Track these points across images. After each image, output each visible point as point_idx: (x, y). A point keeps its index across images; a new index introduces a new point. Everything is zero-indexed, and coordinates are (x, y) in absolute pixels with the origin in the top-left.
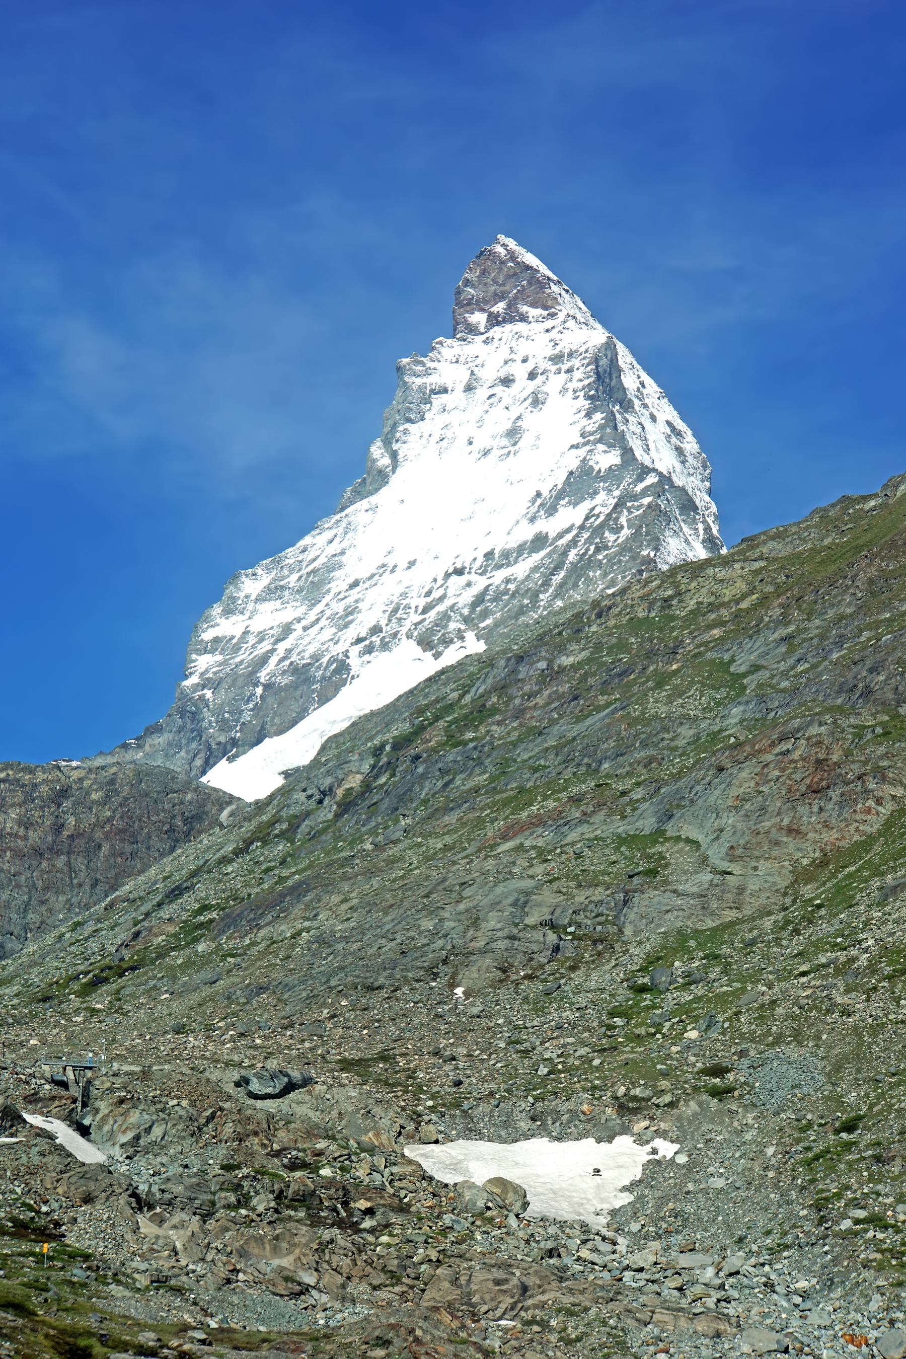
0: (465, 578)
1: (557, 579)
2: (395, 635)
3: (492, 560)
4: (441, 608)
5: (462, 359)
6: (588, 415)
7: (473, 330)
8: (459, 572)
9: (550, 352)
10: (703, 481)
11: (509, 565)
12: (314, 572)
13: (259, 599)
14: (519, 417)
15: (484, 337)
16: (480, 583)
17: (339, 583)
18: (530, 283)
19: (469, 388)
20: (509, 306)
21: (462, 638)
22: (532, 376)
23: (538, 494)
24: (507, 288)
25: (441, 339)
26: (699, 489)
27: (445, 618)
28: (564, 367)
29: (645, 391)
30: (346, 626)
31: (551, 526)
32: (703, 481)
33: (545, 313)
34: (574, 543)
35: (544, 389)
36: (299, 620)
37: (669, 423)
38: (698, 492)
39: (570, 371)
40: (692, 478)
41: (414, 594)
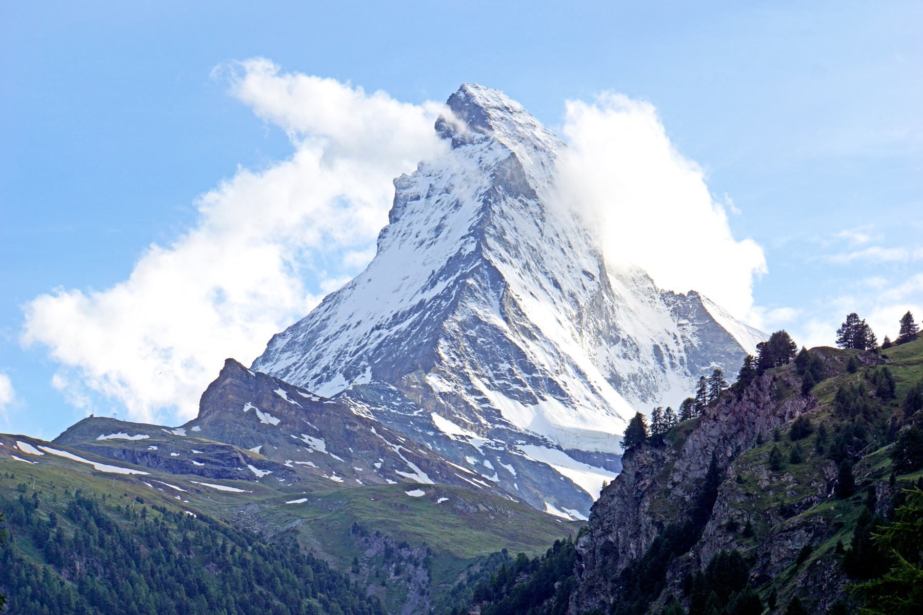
0: (381, 331)
1: (414, 331)
2: (334, 372)
3: (397, 319)
4: (360, 353)
6: (478, 215)
11: (402, 322)
14: (444, 218)
16: (385, 333)
17: (320, 340)
19: (428, 197)
21: (364, 371)
23: (433, 272)
27: (361, 358)
30: (313, 367)
31: (429, 295)
34: (431, 306)
36: (294, 364)
41: (352, 344)
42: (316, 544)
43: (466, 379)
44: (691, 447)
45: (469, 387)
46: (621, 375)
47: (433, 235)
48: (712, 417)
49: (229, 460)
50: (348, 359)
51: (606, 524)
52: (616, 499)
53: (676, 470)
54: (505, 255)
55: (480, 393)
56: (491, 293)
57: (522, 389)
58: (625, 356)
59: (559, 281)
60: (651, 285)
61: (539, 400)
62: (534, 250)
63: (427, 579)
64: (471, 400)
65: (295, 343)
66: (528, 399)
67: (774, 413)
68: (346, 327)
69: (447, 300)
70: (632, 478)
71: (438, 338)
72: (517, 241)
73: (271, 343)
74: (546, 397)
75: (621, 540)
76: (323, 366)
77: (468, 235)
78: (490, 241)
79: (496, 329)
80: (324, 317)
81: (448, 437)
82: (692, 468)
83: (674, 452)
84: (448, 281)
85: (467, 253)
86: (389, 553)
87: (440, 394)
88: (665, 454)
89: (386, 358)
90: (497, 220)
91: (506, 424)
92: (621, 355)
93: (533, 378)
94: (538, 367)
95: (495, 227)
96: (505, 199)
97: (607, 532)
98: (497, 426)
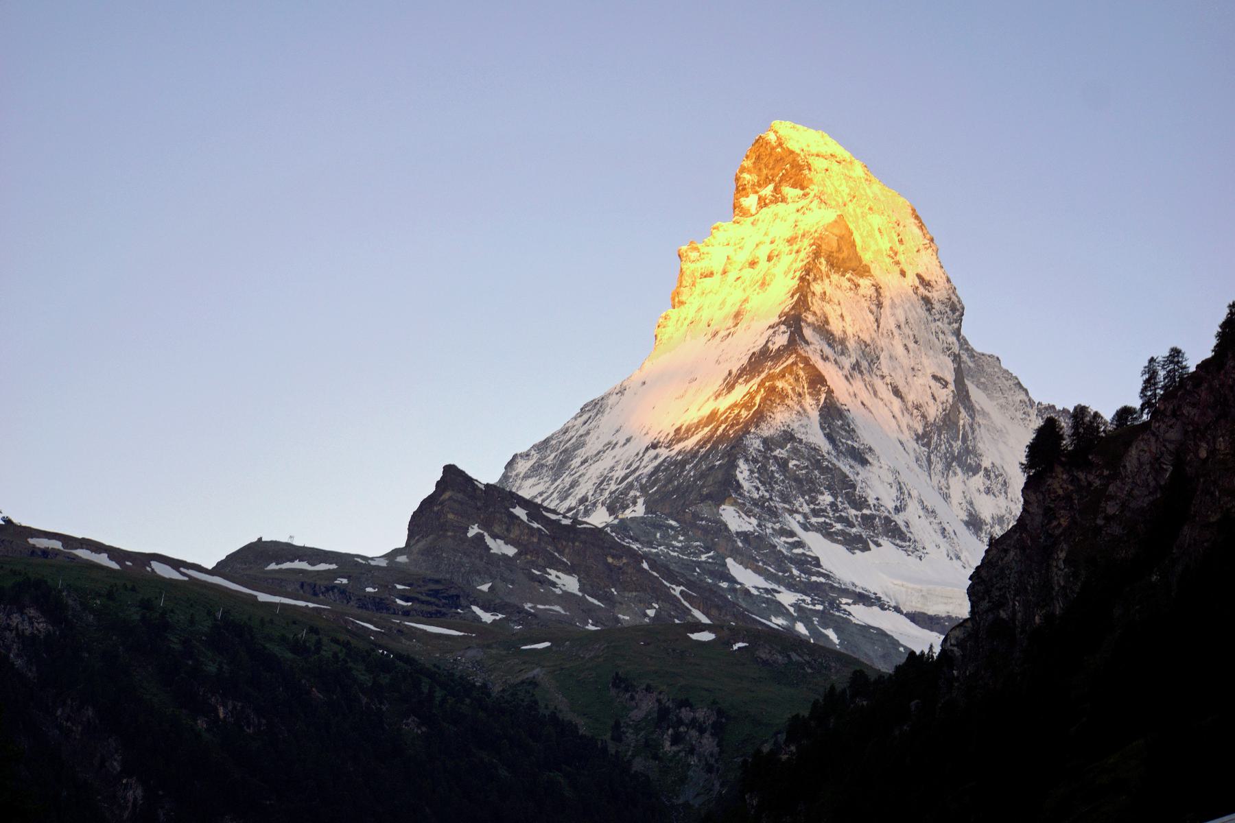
0: (658, 450)
2: (594, 504)
4: (630, 479)
5: (732, 243)
6: (792, 296)
7: (745, 213)
8: (654, 446)
9: (789, 235)
10: (950, 324)
11: (687, 438)
12: (565, 451)
13: (526, 477)
14: (746, 300)
15: (752, 219)
16: (664, 453)
17: (576, 462)
18: (792, 167)
19: (724, 272)
20: (776, 189)
21: (635, 503)
22: (769, 259)
23: (730, 373)
24: (776, 171)
25: (718, 224)
26: (943, 333)
27: (630, 486)
28: (795, 247)
29: (901, 249)
30: (566, 498)
31: (724, 403)
32: (950, 324)
33: (800, 192)
34: (727, 418)
35: (773, 271)
36: (541, 494)
37: (919, 276)
38: (941, 336)
39: (798, 252)
40: (939, 323)
43: (773, 514)
45: (777, 526)
46: (983, 516)
47: (730, 323)
50: (613, 487)
54: (828, 351)
55: (792, 534)
56: (808, 401)
57: (848, 530)
58: (988, 491)
59: (901, 388)
60: (1023, 397)
61: (872, 545)
62: (867, 345)
64: (780, 542)
65: (542, 465)
66: (855, 543)
68: (611, 445)
69: (749, 409)
71: (736, 459)
72: (845, 332)
73: (510, 465)
74: (880, 541)
76: (579, 496)
77: (778, 324)
78: (808, 332)
79: (815, 449)
80: (581, 432)
81: (747, 592)
84: (750, 385)
85: (776, 347)
87: (737, 533)
89: (665, 486)
90: (816, 304)
91: (827, 576)
92: (982, 489)
93: (864, 517)
94: (871, 502)
95: (815, 314)
96: (828, 277)
98: (814, 578)
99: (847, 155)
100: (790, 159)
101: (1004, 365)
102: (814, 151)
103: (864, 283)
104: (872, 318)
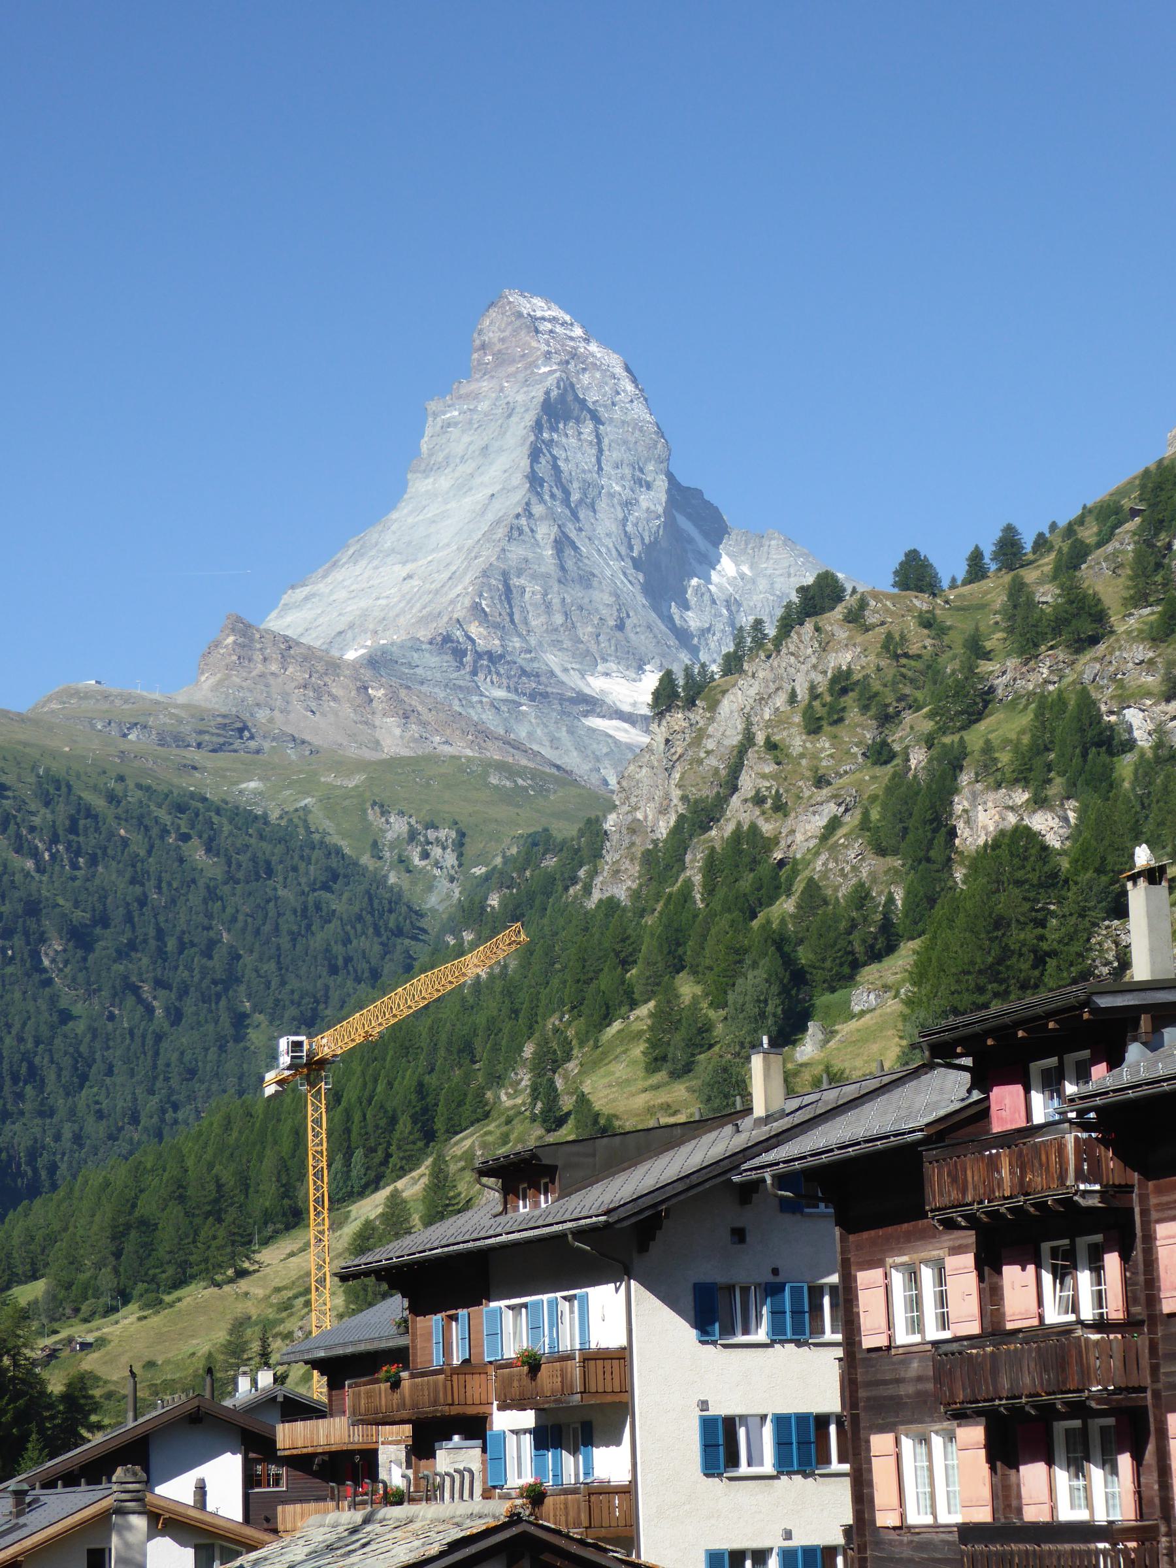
24: (507, 333)
42: (328, 825)
44: (727, 710)
48: (750, 674)
49: (232, 730)
51: (633, 800)
52: (644, 770)
53: (709, 736)
63: (456, 863)
67: (814, 667)
70: (662, 746)
75: (650, 817)
82: (727, 733)
83: (708, 715)
86: (412, 836)
88: (698, 718)
97: (636, 808)
99: (568, 318)
100: (518, 323)
101: (706, 497)
102: (539, 314)
103: (588, 428)
104: (594, 460)
